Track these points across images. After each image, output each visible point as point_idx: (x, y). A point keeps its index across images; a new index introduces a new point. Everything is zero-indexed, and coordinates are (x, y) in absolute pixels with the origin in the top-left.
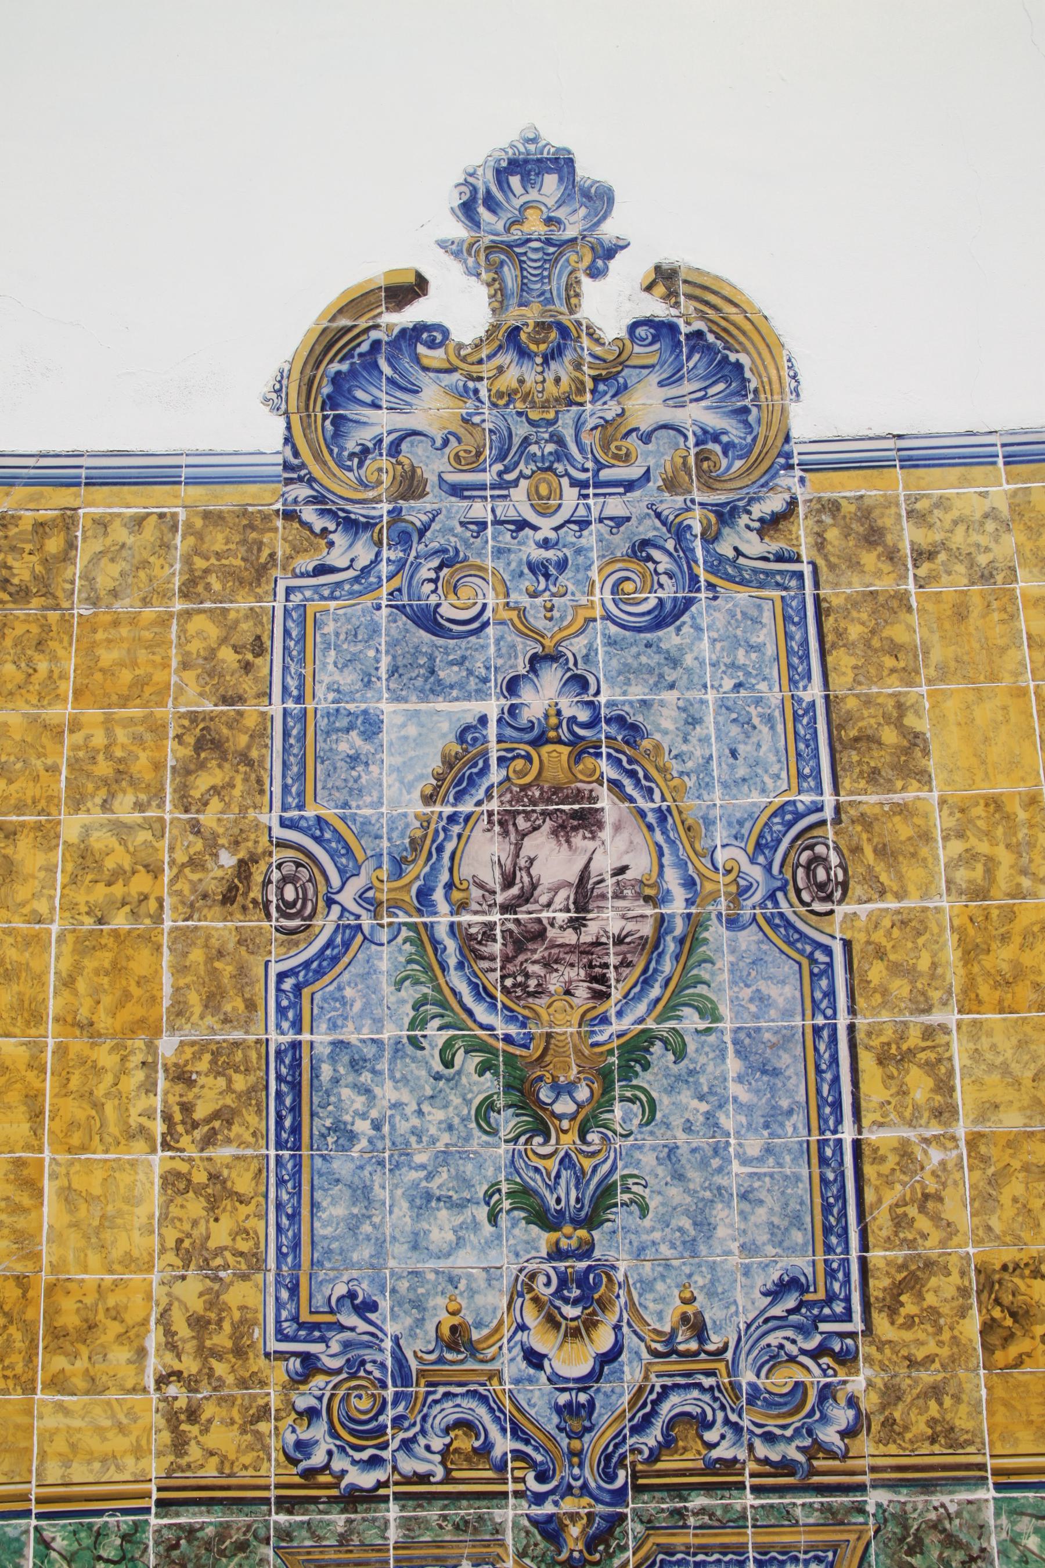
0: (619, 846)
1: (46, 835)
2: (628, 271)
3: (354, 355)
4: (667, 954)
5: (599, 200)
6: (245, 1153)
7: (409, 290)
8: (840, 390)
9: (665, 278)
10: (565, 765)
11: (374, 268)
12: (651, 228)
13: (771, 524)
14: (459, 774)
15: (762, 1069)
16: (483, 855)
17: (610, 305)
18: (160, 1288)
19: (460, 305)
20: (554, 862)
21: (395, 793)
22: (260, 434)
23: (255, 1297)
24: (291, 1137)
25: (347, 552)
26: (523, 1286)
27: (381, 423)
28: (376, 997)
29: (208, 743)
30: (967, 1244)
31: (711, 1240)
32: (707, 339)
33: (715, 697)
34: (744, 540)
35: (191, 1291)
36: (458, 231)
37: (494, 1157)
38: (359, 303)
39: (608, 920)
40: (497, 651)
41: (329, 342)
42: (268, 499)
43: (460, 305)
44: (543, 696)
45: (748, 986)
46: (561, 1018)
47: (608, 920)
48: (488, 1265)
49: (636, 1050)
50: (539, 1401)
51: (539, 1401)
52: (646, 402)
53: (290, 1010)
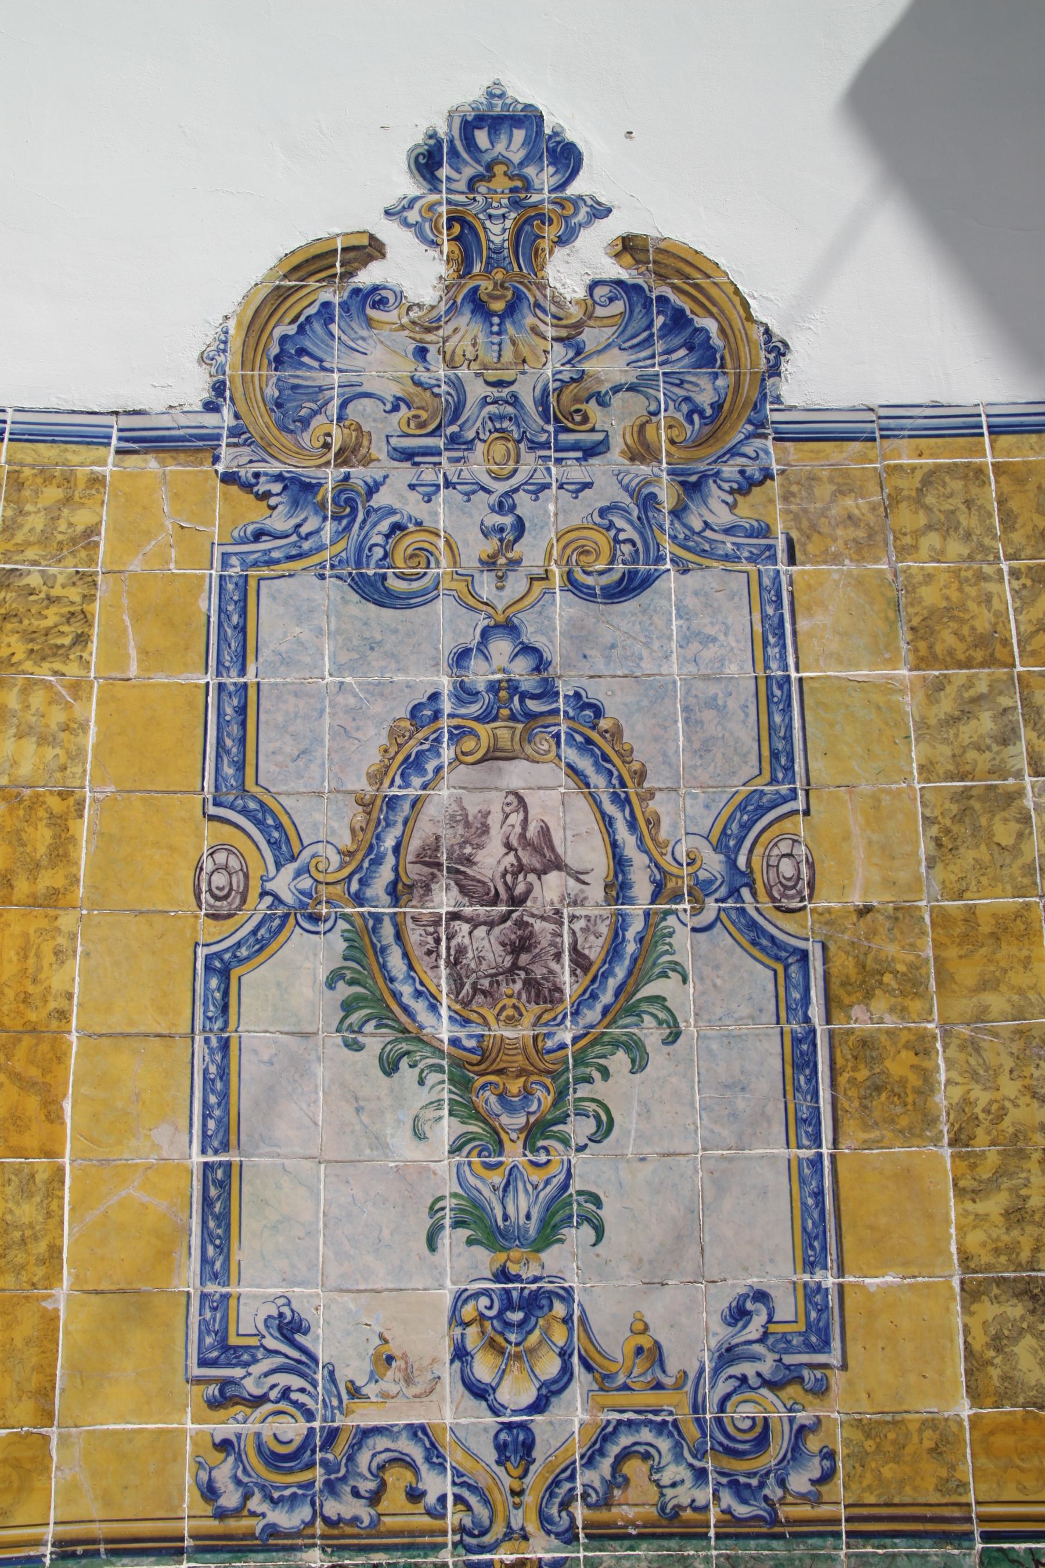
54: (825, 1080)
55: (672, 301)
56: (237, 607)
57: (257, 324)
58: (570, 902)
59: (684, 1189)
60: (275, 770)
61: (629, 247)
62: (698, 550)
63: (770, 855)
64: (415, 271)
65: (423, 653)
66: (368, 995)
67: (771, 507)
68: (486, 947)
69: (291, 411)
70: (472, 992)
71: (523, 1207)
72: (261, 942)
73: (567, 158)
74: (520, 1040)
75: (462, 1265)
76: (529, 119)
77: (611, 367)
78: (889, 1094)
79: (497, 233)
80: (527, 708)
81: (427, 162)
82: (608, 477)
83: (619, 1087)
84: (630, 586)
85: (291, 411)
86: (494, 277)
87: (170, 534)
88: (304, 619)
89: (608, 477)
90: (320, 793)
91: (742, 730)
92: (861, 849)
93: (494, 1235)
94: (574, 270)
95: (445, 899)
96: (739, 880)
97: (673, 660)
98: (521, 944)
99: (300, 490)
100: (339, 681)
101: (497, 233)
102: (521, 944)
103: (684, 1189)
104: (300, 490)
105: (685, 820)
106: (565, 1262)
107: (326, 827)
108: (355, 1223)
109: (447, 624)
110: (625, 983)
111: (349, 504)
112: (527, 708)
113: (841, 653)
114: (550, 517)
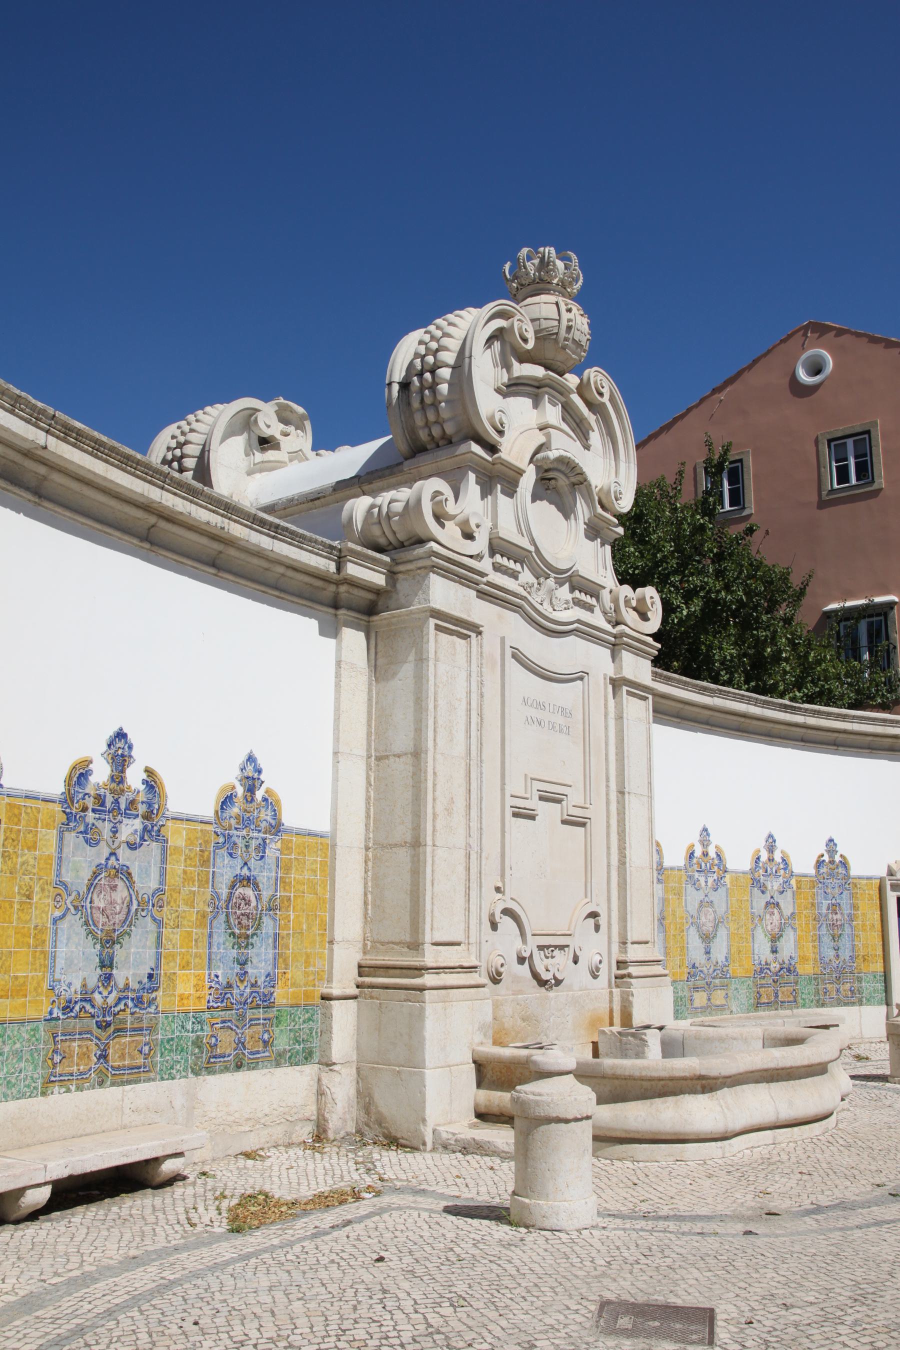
0: (839, 916)
2: (839, 854)
3: (819, 864)
4: (842, 925)
5: (835, 845)
6: (817, 943)
10: (834, 908)
11: (820, 853)
12: (841, 850)
14: (828, 909)
16: (830, 916)
17: (837, 858)
18: (812, 956)
20: (835, 917)
21: (824, 911)
23: (818, 956)
25: (820, 885)
27: (822, 871)
28: (824, 930)
32: (844, 864)
33: (845, 901)
34: (847, 886)
40: (830, 896)
41: (818, 861)
42: (815, 879)
43: (826, 858)
44: (834, 901)
45: (847, 930)
47: (839, 923)
48: (832, 953)
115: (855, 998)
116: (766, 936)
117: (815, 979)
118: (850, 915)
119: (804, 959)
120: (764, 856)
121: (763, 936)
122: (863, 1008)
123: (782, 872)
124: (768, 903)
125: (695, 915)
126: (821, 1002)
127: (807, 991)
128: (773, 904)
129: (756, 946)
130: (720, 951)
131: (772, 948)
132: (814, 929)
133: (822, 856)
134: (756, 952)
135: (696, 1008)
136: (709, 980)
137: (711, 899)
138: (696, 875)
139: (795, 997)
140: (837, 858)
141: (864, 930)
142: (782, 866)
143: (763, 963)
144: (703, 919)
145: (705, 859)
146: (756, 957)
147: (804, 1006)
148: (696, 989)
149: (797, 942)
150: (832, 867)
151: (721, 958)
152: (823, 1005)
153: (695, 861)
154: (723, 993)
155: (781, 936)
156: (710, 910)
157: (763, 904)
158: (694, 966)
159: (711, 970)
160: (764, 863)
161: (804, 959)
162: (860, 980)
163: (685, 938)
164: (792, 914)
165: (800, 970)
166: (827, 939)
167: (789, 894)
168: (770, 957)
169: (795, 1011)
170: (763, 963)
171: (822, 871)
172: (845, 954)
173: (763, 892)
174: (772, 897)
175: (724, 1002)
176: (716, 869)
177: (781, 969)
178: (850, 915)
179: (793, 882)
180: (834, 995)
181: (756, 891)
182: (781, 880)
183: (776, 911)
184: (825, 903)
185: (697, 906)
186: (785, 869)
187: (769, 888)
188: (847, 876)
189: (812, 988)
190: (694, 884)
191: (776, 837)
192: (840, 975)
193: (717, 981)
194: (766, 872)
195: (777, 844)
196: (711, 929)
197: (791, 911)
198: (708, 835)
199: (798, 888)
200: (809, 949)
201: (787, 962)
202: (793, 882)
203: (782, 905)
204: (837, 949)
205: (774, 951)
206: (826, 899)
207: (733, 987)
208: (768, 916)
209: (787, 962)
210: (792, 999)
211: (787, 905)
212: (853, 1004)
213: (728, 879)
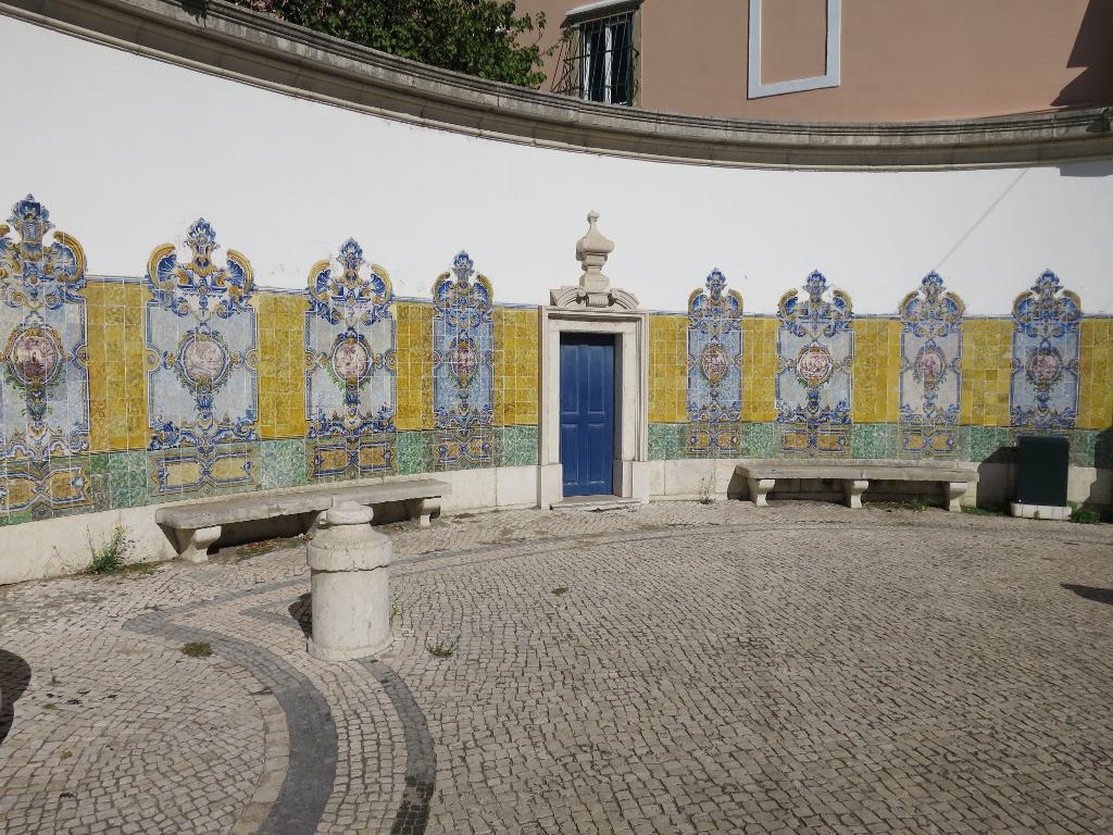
0: (470, 355)
1: (408, 351)
2: (475, 275)
3: (442, 285)
5: (471, 262)
7: (448, 276)
8: (499, 296)
9: (479, 277)
10: (464, 344)
12: (478, 268)
13: (489, 314)
15: (484, 381)
16: (456, 355)
17: (472, 280)
18: (423, 406)
19: (454, 279)
20: (463, 356)
21: (446, 347)
22: (427, 294)
24: (436, 388)
25: (441, 314)
26: (459, 406)
27: (444, 296)
29: (426, 339)
30: (504, 400)
31: (478, 402)
32: (483, 287)
33: (482, 337)
35: (425, 407)
36: (453, 266)
37: (457, 390)
38: (442, 277)
39: (469, 363)
41: (438, 283)
43: (454, 279)
44: (462, 336)
45: (483, 372)
46: (464, 375)
47: (469, 363)
48: (456, 403)
49: (471, 380)
50: (460, 418)
51: (460, 418)
52: (476, 296)
53: (436, 374)
54: (962, 386)
55: (953, 302)
56: (903, 336)
57: (904, 304)
58: (937, 368)
59: (946, 395)
60: (907, 354)
61: (948, 294)
62: (953, 331)
63: (958, 364)
64: (922, 296)
65: (922, 342)
66: (917, 377)
67: (961, 327)
68: (928, 372)
69: (908, 314)
70: (926, 376)
71: (930, 396)
72: (906, 370)
73: (941, 281)
74: (931, 379)
75: (925, 400)
76: (937, 276)
77: (945, 310)
78: (967, 387)
79: (932, 292)
80: (933, 348)
81: (924, 282)
82: (943, 323)
83: (940, 385)
84: (945, 335)
85: (908, 314)
86: (931, 299)
87: (895, 330)
88: (910, 337)
89: (943, 323)
90: (911, 355)
91: (956, 351)
92: (968, 362)
93: (926, 397)
94: (943, 295)
95: (924, 367)
96: (954, 366)
97: (949, 344)
98: (931, 372)
99: (909, 324)
100: (913, 344)
101: (932, 292)
102: (931, 372)
103: (946, 395)
104: (909, 324)
105: (949, 360)
106: (934, 400)
107: (912, 360)
108: (914, 395)
109: (925, 339)
110: (942, 374)
111: (915, 325)
112: (933, 348)
113: (968, 344)
114: (936, 327)
115: (491, 457)
116: (336, 380)
117: (426, 436)
118: (488, 354)
119: (406, 411)
120: (338, 271)
121: (330, 380)
122: (500, 470)
123: (372, 295)
124: (341, 338)
125: (174, 350)
126: (435, 463)
127: (409, 451)
128: (351, 338)
129: (315, 395)
130: (234, 401)
131: (348, 397)
132: (427, 370)
133: (448, 276)
134: (314, 403)
135: (173, 488)
136: (206, 445)
137: (214, 328)
138: (179, 293)
139: (388, 461)
140: (472, 280)
141: (509, 373)
142: (372, 287)
143: (329, 417)
144: (194, 357)
145: (203, 271)
146: (314, 410)
147: (404, 471)
148: (177, 459)
149: (398, 388)
150: (463, 290)
151: (237, 413)
152: (438, 468)
153: (175, 271)
154: (242, 462)
155: (368, 380)
156: (214, 346)
157: (333, 337)
158: (168, 427)
159: (212, 432)
160: (336, 282)
161: (406, 411)
162: (498, 435)
163: (146, 385)
164: (389, 351)
165: (399, 424)
166: (448, 385)
167: (385, 325)
168: (344, 410)
169: (387, 478)
170: (329, 417)
171: (444, 296)
172: (478, 402)
173: (333, 322)
174: (350, 329)
175: (244, 474)
176: (228, 285)
177: (365, 424)
178: (488, 354)
179: (393, 309)
180: (457, 453)
181: (318, 320)
182: (370, 306)
183: (357, 348)
184: (448, 339)
185: (178, 338)
186: (377, 291)
187: (346, 316)
188: (486, 304)
189: (420, 447)
190: (174, 306)
191: (361, 246)
192: (469, 429)
193: (227, 447)
194: (341, 293)
195: (364, 255)
196: (214, 373)
197: (389, 346)
198: (212, 235)
199: (400, 316)
200: (417, 398)
201: (375, 414)
202: (393, 309)
203: (370, 340)
204: (464, 397)
205: (351, 400)
206: (449, 332)
207: (263, 452)
208: (341, 355)
209: (375, 414)
210: (383, 462)
211: (380, 339)
212: (486, 465)
213: (255, 301)
